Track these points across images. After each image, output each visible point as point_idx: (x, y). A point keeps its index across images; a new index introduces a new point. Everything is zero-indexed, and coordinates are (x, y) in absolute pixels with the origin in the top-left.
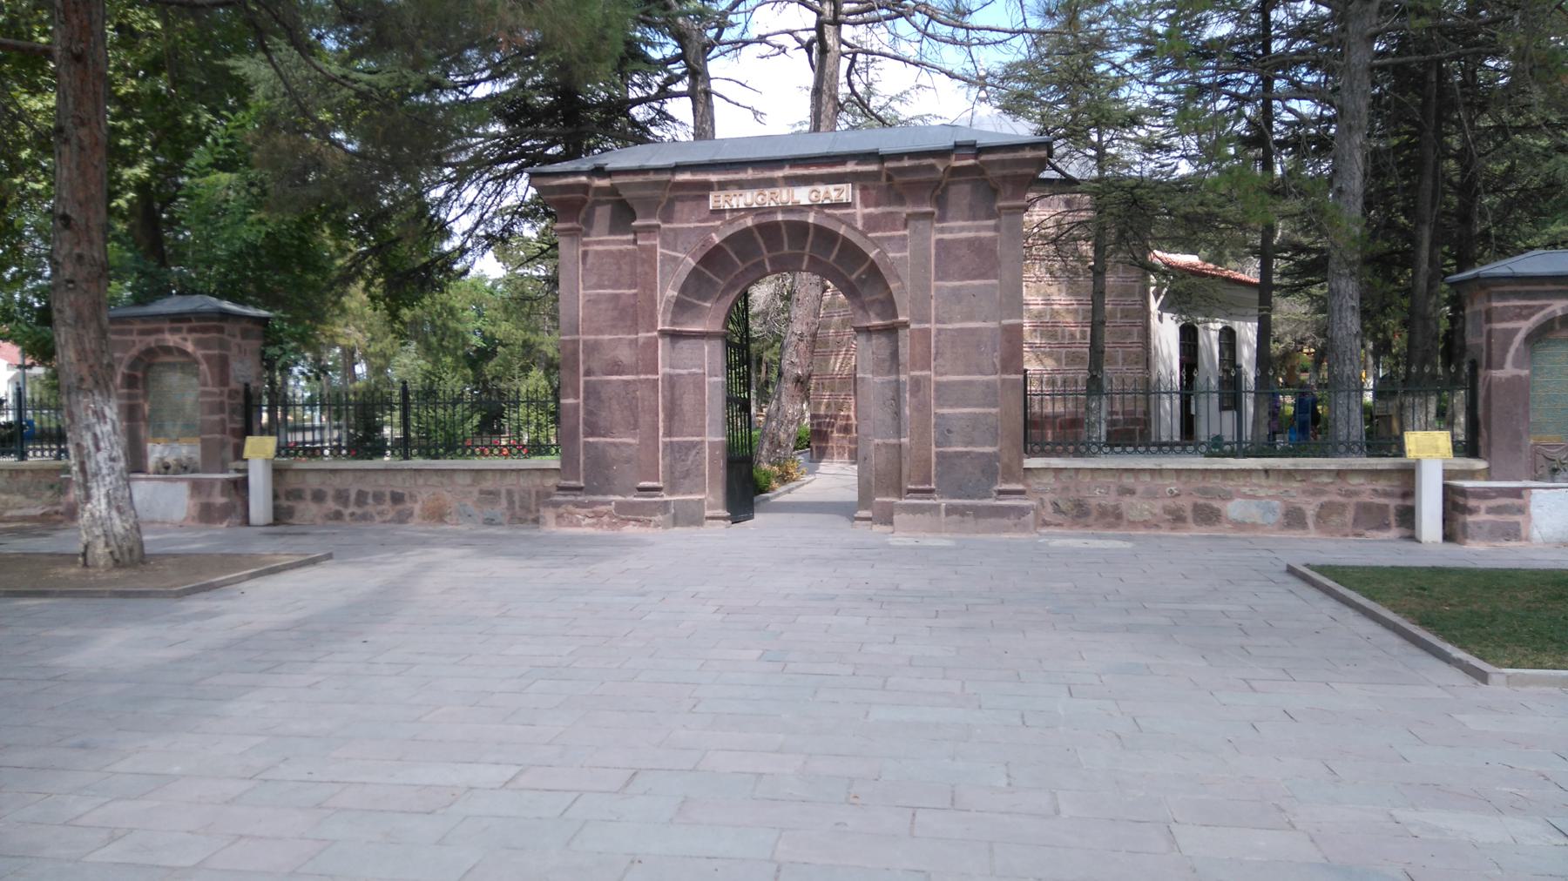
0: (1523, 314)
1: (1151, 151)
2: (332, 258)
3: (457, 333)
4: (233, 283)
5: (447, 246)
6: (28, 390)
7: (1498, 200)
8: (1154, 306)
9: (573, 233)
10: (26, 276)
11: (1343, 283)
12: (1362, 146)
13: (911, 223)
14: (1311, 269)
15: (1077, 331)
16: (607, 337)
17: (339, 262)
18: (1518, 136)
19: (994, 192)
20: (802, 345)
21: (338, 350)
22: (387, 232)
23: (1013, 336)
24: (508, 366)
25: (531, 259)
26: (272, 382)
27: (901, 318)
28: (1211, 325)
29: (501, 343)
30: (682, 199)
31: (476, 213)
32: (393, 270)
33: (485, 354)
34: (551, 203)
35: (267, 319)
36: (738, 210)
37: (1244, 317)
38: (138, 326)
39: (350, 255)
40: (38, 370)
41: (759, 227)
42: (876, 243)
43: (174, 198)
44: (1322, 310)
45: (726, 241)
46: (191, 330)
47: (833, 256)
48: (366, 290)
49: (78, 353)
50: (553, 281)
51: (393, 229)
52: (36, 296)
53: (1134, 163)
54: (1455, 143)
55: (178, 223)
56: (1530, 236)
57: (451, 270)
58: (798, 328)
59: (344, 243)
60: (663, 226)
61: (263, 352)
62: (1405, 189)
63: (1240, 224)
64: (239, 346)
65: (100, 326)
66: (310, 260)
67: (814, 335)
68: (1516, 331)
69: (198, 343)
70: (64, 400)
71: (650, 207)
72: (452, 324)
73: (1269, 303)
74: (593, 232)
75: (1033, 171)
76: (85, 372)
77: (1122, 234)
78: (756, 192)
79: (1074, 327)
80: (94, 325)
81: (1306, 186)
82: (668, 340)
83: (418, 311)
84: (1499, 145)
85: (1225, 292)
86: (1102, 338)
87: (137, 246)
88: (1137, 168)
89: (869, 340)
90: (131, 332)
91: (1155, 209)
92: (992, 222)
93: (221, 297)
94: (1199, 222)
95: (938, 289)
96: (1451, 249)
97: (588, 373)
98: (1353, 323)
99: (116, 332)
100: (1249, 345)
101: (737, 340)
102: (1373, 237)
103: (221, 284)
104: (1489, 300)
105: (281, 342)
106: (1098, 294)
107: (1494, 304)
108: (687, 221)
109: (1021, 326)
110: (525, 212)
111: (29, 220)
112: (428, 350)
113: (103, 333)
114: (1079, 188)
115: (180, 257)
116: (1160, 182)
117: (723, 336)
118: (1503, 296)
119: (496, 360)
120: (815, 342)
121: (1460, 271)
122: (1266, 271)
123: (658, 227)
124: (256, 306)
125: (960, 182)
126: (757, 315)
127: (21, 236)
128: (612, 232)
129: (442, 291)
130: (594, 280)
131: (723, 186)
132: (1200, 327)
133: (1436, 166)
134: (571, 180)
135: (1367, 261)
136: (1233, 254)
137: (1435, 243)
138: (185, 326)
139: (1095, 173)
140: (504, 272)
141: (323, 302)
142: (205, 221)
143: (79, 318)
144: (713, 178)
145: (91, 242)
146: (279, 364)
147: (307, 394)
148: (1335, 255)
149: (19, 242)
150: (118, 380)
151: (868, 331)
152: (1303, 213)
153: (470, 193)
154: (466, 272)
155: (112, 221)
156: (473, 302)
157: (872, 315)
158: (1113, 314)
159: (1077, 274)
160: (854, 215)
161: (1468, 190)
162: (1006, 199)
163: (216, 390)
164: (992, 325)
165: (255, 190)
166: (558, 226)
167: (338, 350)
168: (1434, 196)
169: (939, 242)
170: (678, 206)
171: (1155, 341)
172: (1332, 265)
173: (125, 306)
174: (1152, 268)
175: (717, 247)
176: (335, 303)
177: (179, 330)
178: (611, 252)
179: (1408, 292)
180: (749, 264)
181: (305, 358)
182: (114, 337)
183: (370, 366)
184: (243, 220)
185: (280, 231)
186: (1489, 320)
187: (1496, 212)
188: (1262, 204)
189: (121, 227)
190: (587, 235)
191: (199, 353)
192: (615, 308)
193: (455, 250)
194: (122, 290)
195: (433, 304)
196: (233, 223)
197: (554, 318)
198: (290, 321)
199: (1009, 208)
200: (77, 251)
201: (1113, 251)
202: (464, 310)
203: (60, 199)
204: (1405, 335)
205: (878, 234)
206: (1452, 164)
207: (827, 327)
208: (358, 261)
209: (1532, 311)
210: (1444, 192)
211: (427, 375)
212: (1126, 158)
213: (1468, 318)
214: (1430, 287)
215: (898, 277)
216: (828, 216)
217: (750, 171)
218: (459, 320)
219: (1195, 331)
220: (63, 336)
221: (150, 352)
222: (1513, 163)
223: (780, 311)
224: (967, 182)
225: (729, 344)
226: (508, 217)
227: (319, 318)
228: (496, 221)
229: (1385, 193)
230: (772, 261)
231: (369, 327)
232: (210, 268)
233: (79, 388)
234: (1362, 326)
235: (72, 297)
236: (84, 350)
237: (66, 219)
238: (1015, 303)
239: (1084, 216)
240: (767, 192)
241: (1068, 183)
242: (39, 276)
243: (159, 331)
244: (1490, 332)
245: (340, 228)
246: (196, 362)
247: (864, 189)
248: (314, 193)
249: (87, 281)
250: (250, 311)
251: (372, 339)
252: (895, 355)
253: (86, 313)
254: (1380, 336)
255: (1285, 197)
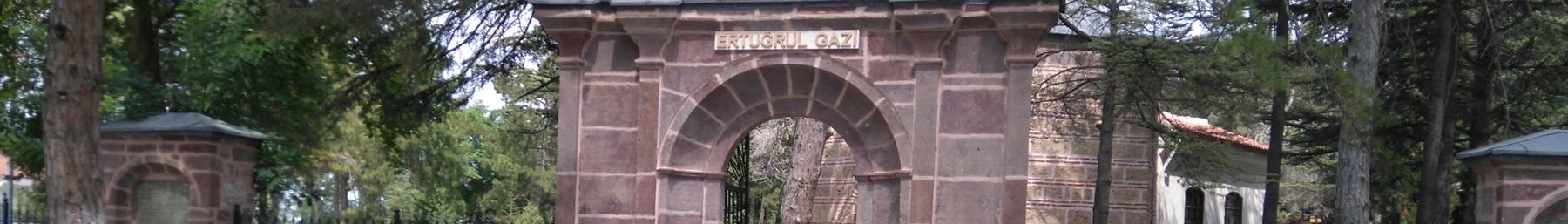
0: (1533, 194)
1: (1165, 11)
2: (329, 82)
3: (452, 163)
4: (228, 102)
5: (447, 75)
6: (15, 201)
7: (1515, 76)
8: (1161, 168)
9: (574, 67)
10: (18, 86)
11: (1353, 154)
12: (1379, 15)
13: (919, 73)
14: (1322, 137)
15: (1082, 191)
16: (604, 175)
17: (336, 86)
18: (1538, 13)
19: (1004, 46)
20: (802, 192)
21: (331, 176)
22: (387, 58)
23: (1017, 192)
24: (503, 199)
25: (531, 92)
26: (263, 205)
27: (904, 169)
28: (1218, 190)
29: (497, 176)
30: (687, 38)
31: (478, 42)
32: (391, 97)
33: (480, 187)
34: (555, 36)
35: (260, 141)
36: (744, 51)
37: (1252, 184)
38: (131, 142)
39: (347, 80)
40: (26, 182)
41: (764, 70)
42: (882, 91)
43: (172, 13)
44: (1331, 180)
45: (729, 82)
46: (183, 149)
47: (837, 103)
48: (362, 115)
49: (67, 166)
50: (552, 115)
51: (392, 55)
52: (27, 106)
53: (1148, 22)
54: (1474, 16)
55: (175, 40)
56: (1546, 115)
57: (449, 99)
58: (799, 174)
59: (343, 67)
60: (667, 64)
61: (255, 175)
62: (1420, 61)
63: (1252, 89)
64: (231, 167)
65: (91, 140)
66: (307, 83)
67: (815, 182)
68: (1526, 211)
69: (189, 162)
70: (51, 214)
71: (655, 44)
72: (448, 154)
73: (1278, 171)
74: (596, 67)
75: (1044, 26)
76: (73, 186)
77: (1131, 95)
78: (762, 34)
79: (1079, 186)
80: (85, 138)
81: (1320, 53)
82: (666, 180)
83: (414, 139)
84: (1518, 20)
85: (1233, 157)
86: (1107, 198)
87: (132, 60)
88: (1150, 27)
89: (870, 190)
90: (121, 148)
91: (1166, 69)
92: (1000, 76)
93: (215, 116)
94: (1210, 84)
95: (943, 141)
96: (1465, 124)
97: (584, 210)
98: (1362, 195)
99: (107, 147)
100: (1256, 212)
101: (736, 184)
102: (1386, 108)
103: (215, 103)
104: (1501, 178)
105: (274, 164)
106: (1105, 154)
107: (1506, 182)
108: (691, 60)
109: (1025, 182)
110: (527, 44)
111: (24, 29)
112: (422, 179)
113: (93, 148)
114: (1090, 45)
115: (175, 74)
116: (1172, 43)
117: (723, 179)
118: (1515, 174)
119: (491, 193)
120: (816, 189)
121: (1472, 146)
122: (1276, 137)
123: (662, 65)
124: (250, 127)
125: (970, 34)
126: (758, 159)
127: (15, 45)
128: (615, 68)
129: (439, 121)
130: (594, 115)
131: (729, 26)
132: (1206, 192)
133: (1454, 38)
134: (575, 13)
135: (1379, 132)
136: (1243, 119)
137: (1449, 117)
138: (177, 144)
139: (1107, 31)
140: (503, 104)
141: (318, 124)
142: (202, 39)
143: (70, 130)
144: (720, 18)
145: (85, 54)
146: (271, 187)
147: (298, 219)
148: (1347, 124)
149: (13, 51)
150: (107, 196)
151: (870, 180)
152: (1316, 81)
153: (472, 22)
154: (464, 102)
155: (108, 34)
156: (470, 132)
157: (875, 164)
158: (1119, 175)
159: (1084, 132)
160: (861, 62)
161: (1484, 64)
162: (1016, 53)
163: (205, 210)
164: (996, 180)
165: (254, 9)
166: (560, 59)
167: (331, 176)
168: (1450, 70)
169: (946, 93)
170: (683, 45)
171: (1160, 204)
172: (1343, 135)
173: (118, 121)
174: (1161, 130)
175: (721, 89)
176: (331, 128)
177: (171, 148)
178: (611, 90)
179: (1419, 166)
180: (751, 107)
181: (297, 182)
182: (104, 152)
183: (363, 193)
184: (240, 39)
185: (278, 52)
186: (1500, 197)
187: (1512, 88)
188: (1275, 69)
189: (117, 40)
190: (589, 70)
191: (190, 172)
192: (613, 146)
193: (454, 79)
194: (114, 104)
195: (430, 133)
196: (231, 42)
197: (552, 153)
198: (283, 144)
199: (1018, 62)
200: (71, 62)
201: (1122, 110)
202: (461, 140)
203: (56, 9)
204: (1414, 209)
205: (885, 83)
206: (1469, 37)
207: (829, 174)
208: (356, 86)
209: (1545, 191)
210: (1461, 66)
211: (420, 205)
212: (1140, 17)
213: (1479, 195)
214: (1442, 161)
215: (903, 128)
216: (834, 61)
217: (757, 13)
218: (455, 151)
219: (1201, 195)
220: (53, 148)
221: (140, 169)
222: (1532, 39)
223: (781, 156)
224: (977, 33)
225: (728, 187)
226: (509, 48)
227: (313, 142)
228: (497, 51)
229: (1400, 64)
230: (775, 105)
231: (364, 153)
232: (205, 86)
233: (67, 202)
234: (1371, 198)
235: (64, 109)
236: (73, 163)
237: (61, 31)
238: (1020, 159)
239: (1094, 73)
240: (773, 35)
241: (1079, 39)
242: (31, 86)
243: (151, 148)
244: (1500, 211)
245: (339, 52)
246: (187, 181)
247: (872, 36)
248: (315, 14)
249: (79, 93)
250: (244, 132)
251: (367, 166)
252: (896, 206)
253: (78, 126)
254: (1389, 209)
255: (1299, 64)
